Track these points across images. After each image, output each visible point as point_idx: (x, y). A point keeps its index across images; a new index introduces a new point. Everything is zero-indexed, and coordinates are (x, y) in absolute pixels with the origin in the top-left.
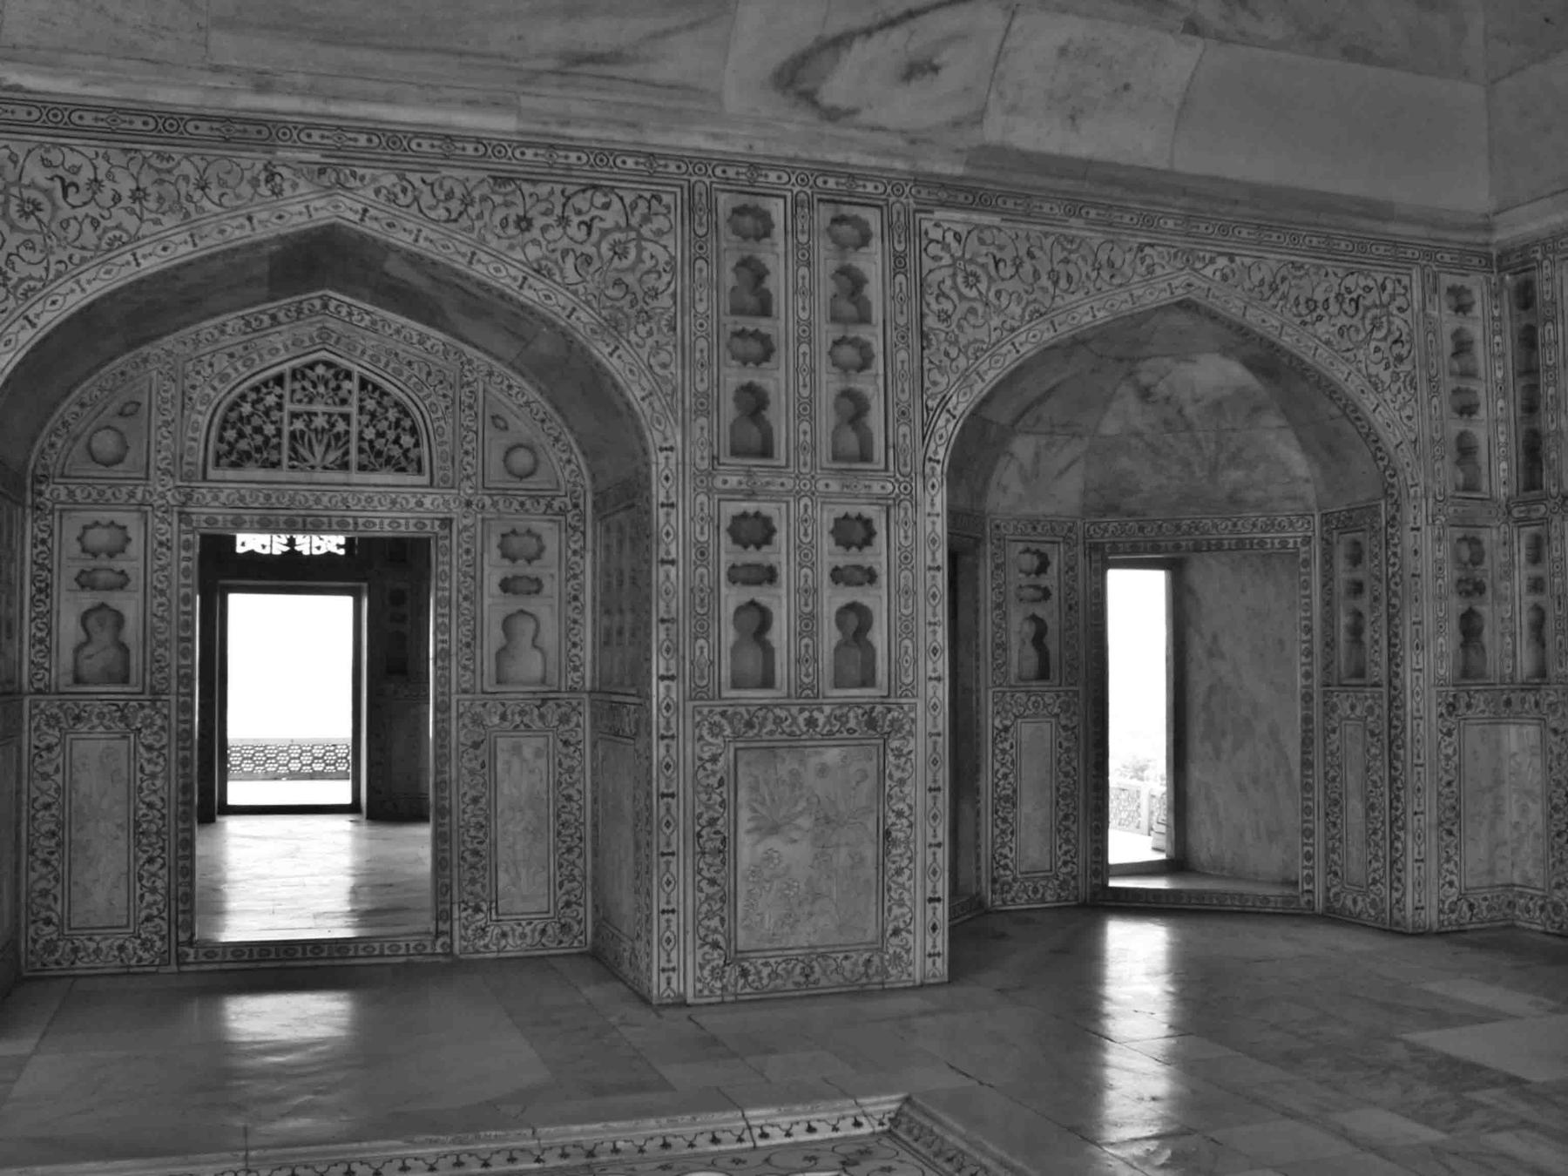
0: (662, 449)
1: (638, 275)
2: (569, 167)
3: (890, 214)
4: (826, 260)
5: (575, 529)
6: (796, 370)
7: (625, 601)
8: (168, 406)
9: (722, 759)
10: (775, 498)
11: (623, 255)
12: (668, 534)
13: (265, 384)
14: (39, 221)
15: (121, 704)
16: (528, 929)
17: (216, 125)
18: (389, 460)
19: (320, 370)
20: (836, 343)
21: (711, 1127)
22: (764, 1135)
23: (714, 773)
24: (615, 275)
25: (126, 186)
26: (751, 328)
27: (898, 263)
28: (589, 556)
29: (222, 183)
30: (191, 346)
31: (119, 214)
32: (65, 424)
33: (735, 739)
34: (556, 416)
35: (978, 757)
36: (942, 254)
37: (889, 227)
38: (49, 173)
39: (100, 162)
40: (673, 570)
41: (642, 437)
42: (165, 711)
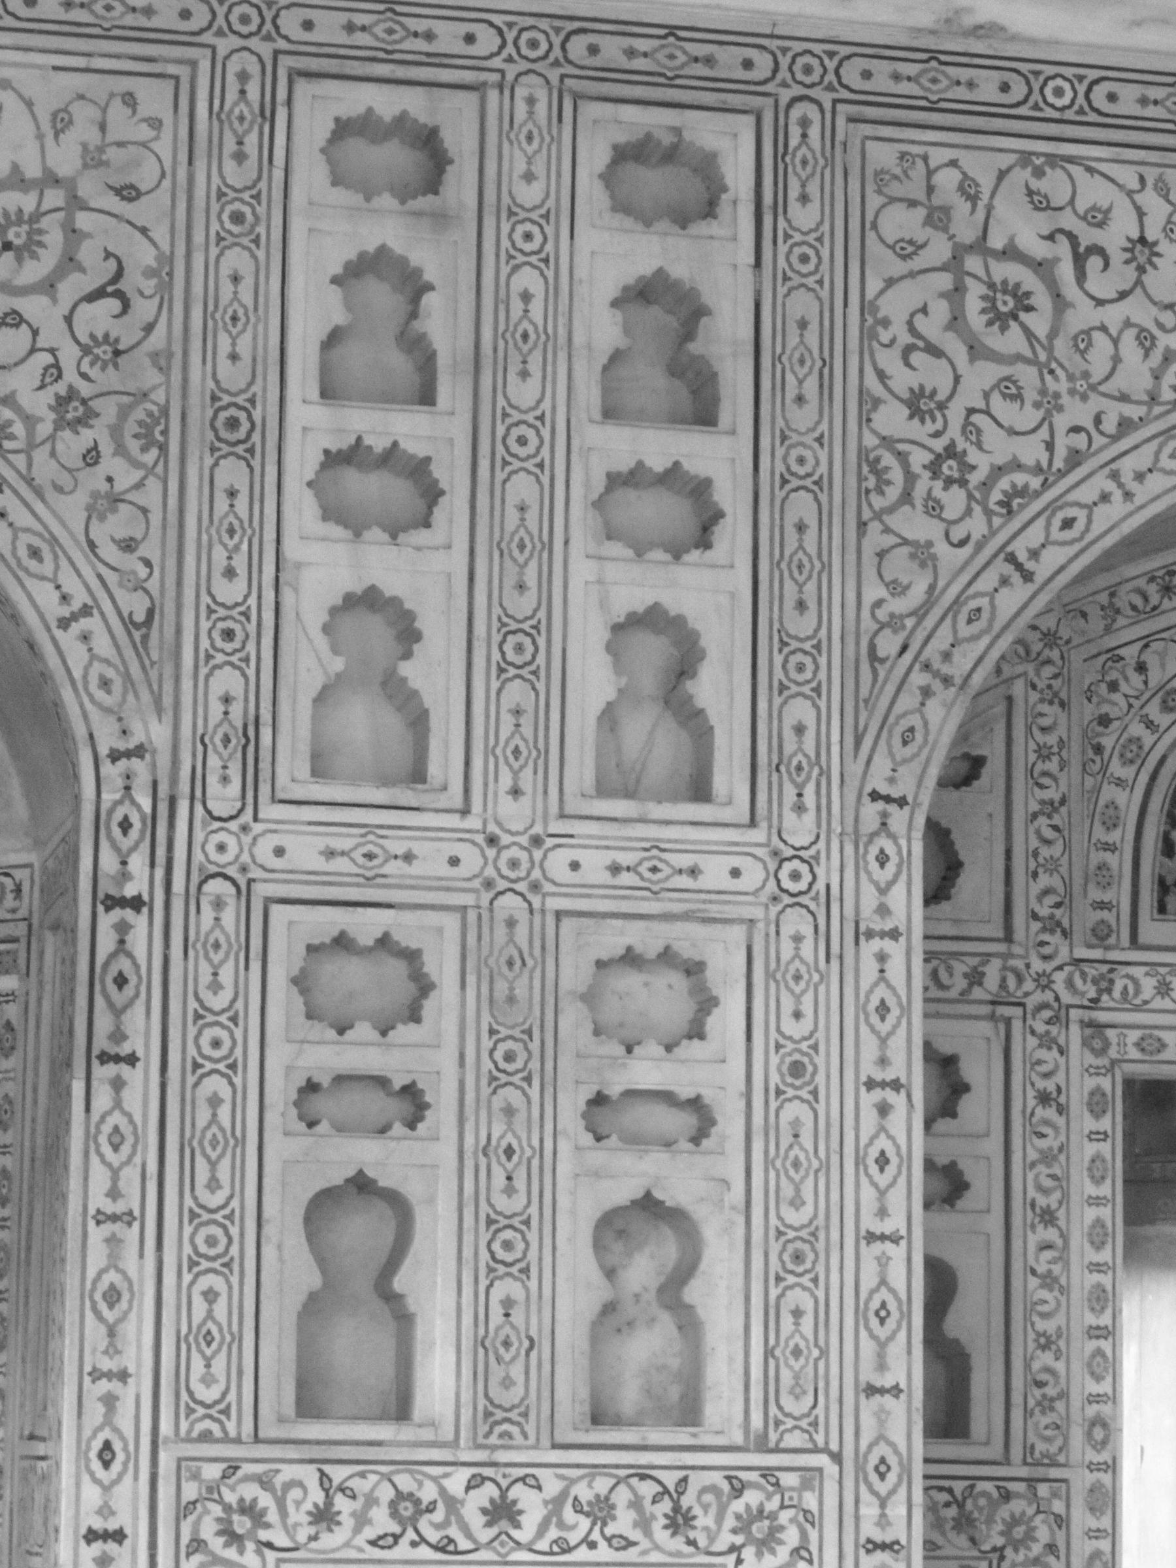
8: (1053, 766)
15: (959, 1487)
30: (1096, 624)
38: (1044, 222)
39: (1150, 200)
42: (1058, 1507)
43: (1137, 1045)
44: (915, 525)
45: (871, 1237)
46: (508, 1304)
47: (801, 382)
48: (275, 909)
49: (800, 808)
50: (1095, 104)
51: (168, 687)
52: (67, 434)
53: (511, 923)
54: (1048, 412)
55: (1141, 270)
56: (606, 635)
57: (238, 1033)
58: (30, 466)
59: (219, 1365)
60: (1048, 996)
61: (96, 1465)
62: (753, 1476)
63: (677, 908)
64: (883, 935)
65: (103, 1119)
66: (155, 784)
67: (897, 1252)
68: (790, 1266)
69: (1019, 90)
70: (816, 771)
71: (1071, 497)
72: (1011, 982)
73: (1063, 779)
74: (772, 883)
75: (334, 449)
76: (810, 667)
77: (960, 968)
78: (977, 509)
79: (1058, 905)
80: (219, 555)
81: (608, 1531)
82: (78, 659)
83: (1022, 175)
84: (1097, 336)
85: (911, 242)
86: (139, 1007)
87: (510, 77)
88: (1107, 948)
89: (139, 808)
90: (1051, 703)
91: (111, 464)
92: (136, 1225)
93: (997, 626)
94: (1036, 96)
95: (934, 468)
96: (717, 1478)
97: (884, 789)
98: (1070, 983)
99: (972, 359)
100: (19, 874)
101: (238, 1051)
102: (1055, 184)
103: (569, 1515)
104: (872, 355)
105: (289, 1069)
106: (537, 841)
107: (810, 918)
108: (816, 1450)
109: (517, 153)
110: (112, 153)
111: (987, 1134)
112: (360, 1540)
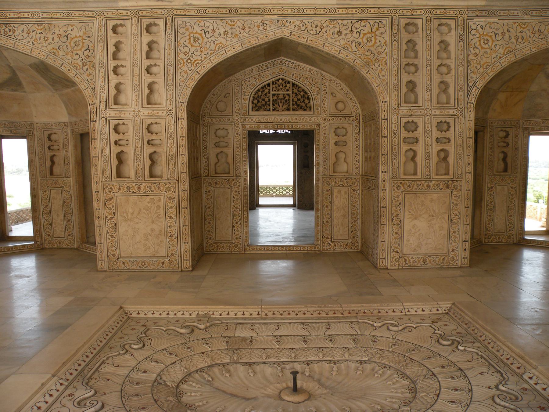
0: (383, 102)
1: (375, 47)
2: (353, 14)
3: (458, 21)
4: (436, 38)
5: (357, 126)
6: (426, 75)
7: (372, 149)
9: (400, 197)
10: (418, 116)
11: (371, 41)
12: (385, 128)
13: (265, 86)
16: (342, 244)
17: (246, 10)
18: (301, 107)
19: (281, 81)
20: (439, 66)
21: (393, 307)
22: (409, 311)
23: (398, 201)
24: (368, 48)
25: (222, 31)
26: (411, 63)
27: (461, 38)
28: (361, 134)
29: (249, 27)
31: (221, 39)
32: (210, 101)
33: (405, 190)
34: (351, 93)
35: (482, 196)
36: (476, 33)
37: (457, 26)
38: (201, 29)
40: (386, 139)
41: (376, 98)
44: (184, 68)
45: (182, 155)
69: (196, 12)
77: (227, 119)
83: (198, 23)
91: (89, 70)
95: (187, 61)
102: (202, 24)
110: (87, 32)
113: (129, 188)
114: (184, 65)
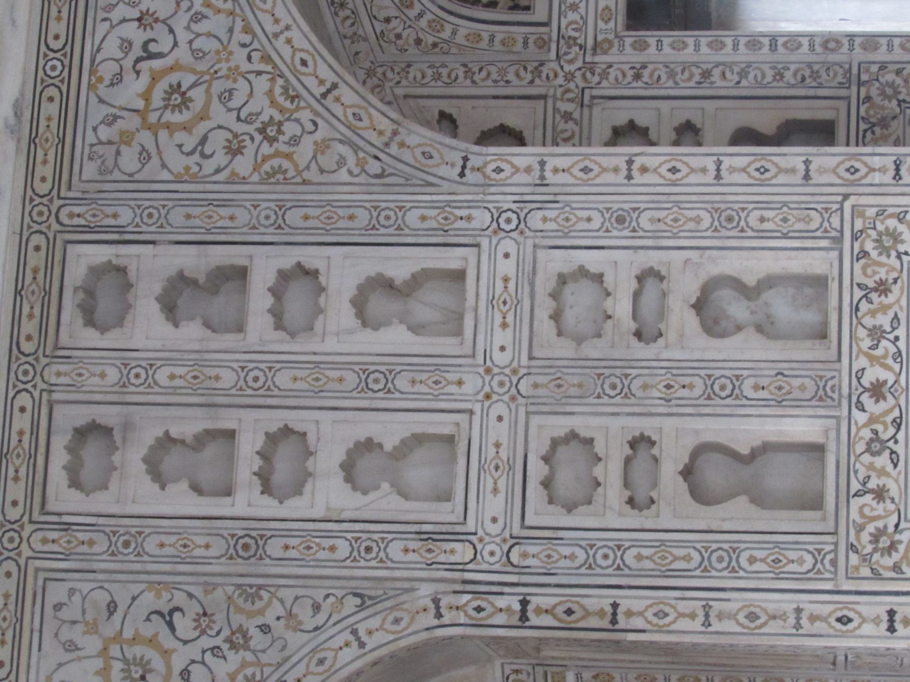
8: (444, 72)
14: (194, 85)
15: (863, 126)
30: (362, 46)
38: (129, 76)
39: (116, 15)
42: (874, 68)
43: (606, 23)
45: (718, 177)
46: (756, 387)
47: (222, 218)
48: (528, 522)
49: (469, 218)
50: (60, 47)
51: (399, 585)
52: (252, 643)
53: (536, 386)
54: (239, 74)
55: (156, 20)
56: (369, 330)
57: (599, 544)
58: (270, 665)
59: (792, 555)
60: (578, 74)
61: (850, 626)
62: (857, 245)
63: (527, 289)
64: (542, 170)
65: (649, 622)
66: (455, 592)
67: (727, 162)
68: (735, 224)
70: (447, 209)
71: (289, 61)
72: (570, 95)
73: (451, 66)
74: (512, 234)
75: (261, 489)
76: (387, 212)
77: (562, 126)
78: (295, 115)
79: (525, 68)
80: (322, 555)
81: (889, 329)
82: (382, 637)
83: (102, 90)
84: (195, 45)
85: (141, 154)
86: (585, 601)
87: (45, 386)
88: (550, 40)
89: (468, 602)
90: (408, 73)
91: (269, 618)
92: (711, 603)
93: (363, 104)
94: (56, 81)
95: (272, 140)
96: (858, 266)
97: (458, 170)
98: (571, 62)
99: (209, 118)
100: (507, 672)
101: (610, 544)
102: (107, 70)
103: (879, 352)
104: (206, 176)
105: (620, 514)
106: (488, 371)
107: (533, 212)
108: (841, 209)
109: (88, 382)
110: (89, 617)
111: (659, 110)
112: (894, 473)
113: (876, 445)
114: (288, 156)
